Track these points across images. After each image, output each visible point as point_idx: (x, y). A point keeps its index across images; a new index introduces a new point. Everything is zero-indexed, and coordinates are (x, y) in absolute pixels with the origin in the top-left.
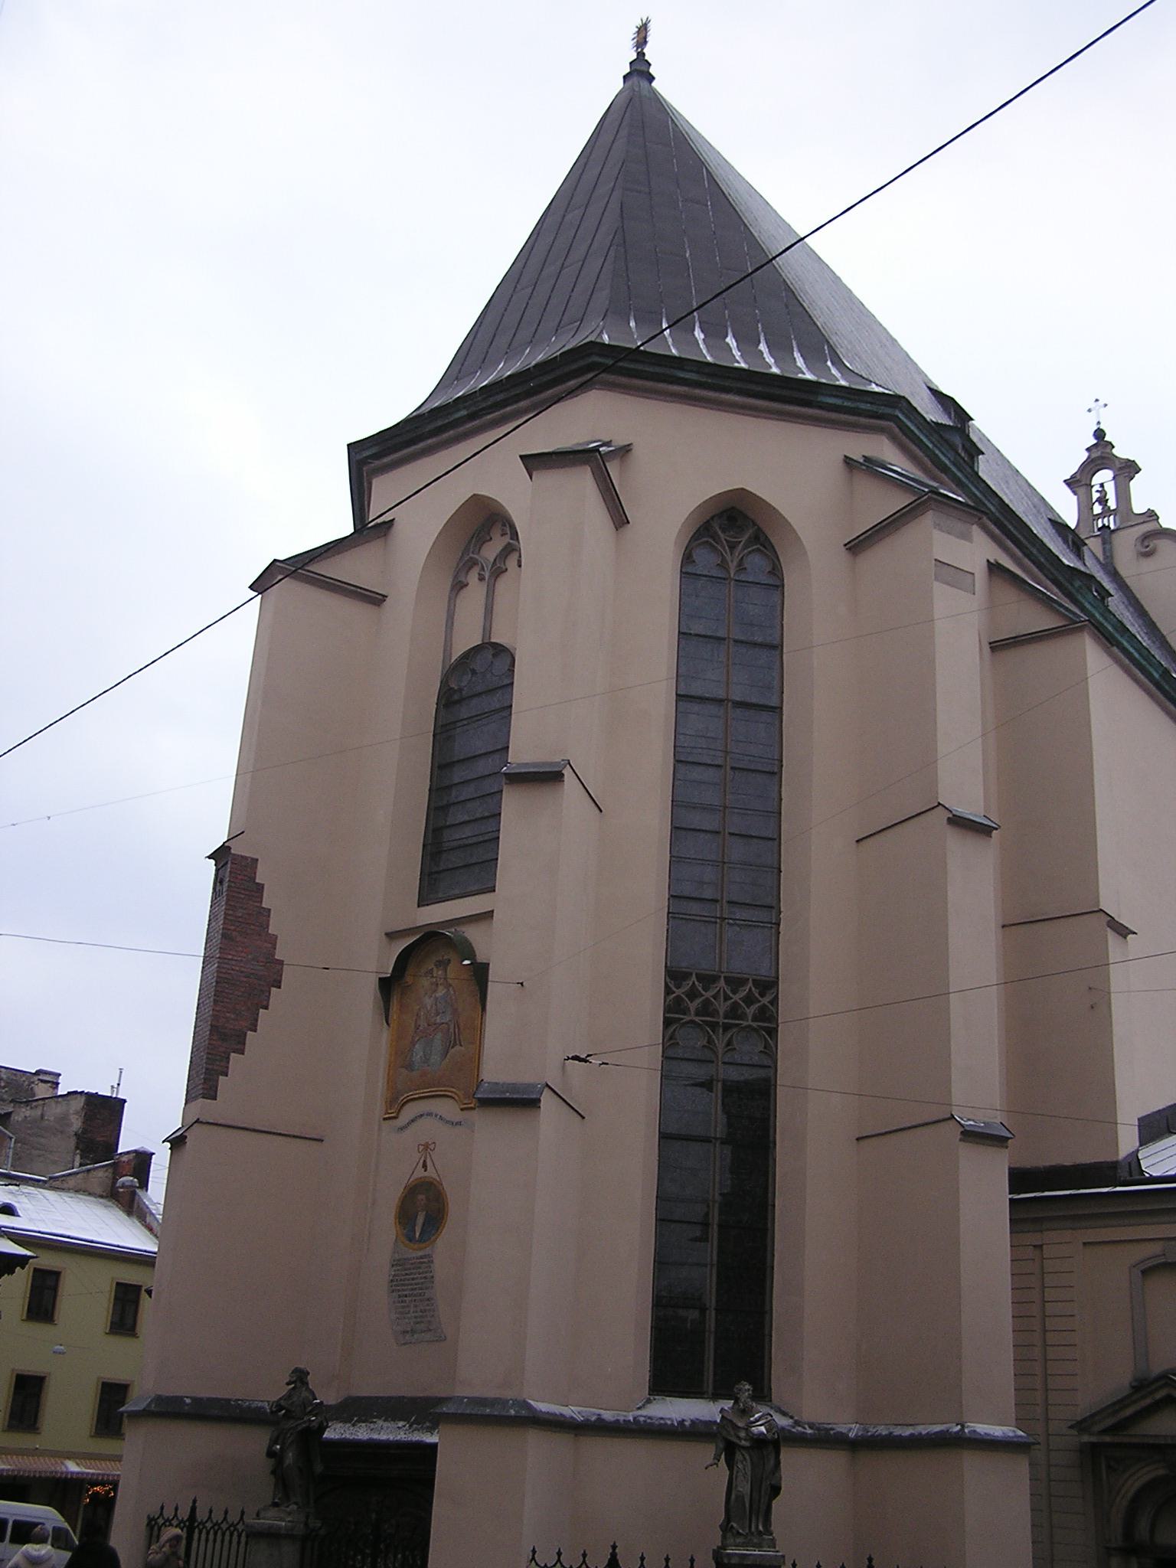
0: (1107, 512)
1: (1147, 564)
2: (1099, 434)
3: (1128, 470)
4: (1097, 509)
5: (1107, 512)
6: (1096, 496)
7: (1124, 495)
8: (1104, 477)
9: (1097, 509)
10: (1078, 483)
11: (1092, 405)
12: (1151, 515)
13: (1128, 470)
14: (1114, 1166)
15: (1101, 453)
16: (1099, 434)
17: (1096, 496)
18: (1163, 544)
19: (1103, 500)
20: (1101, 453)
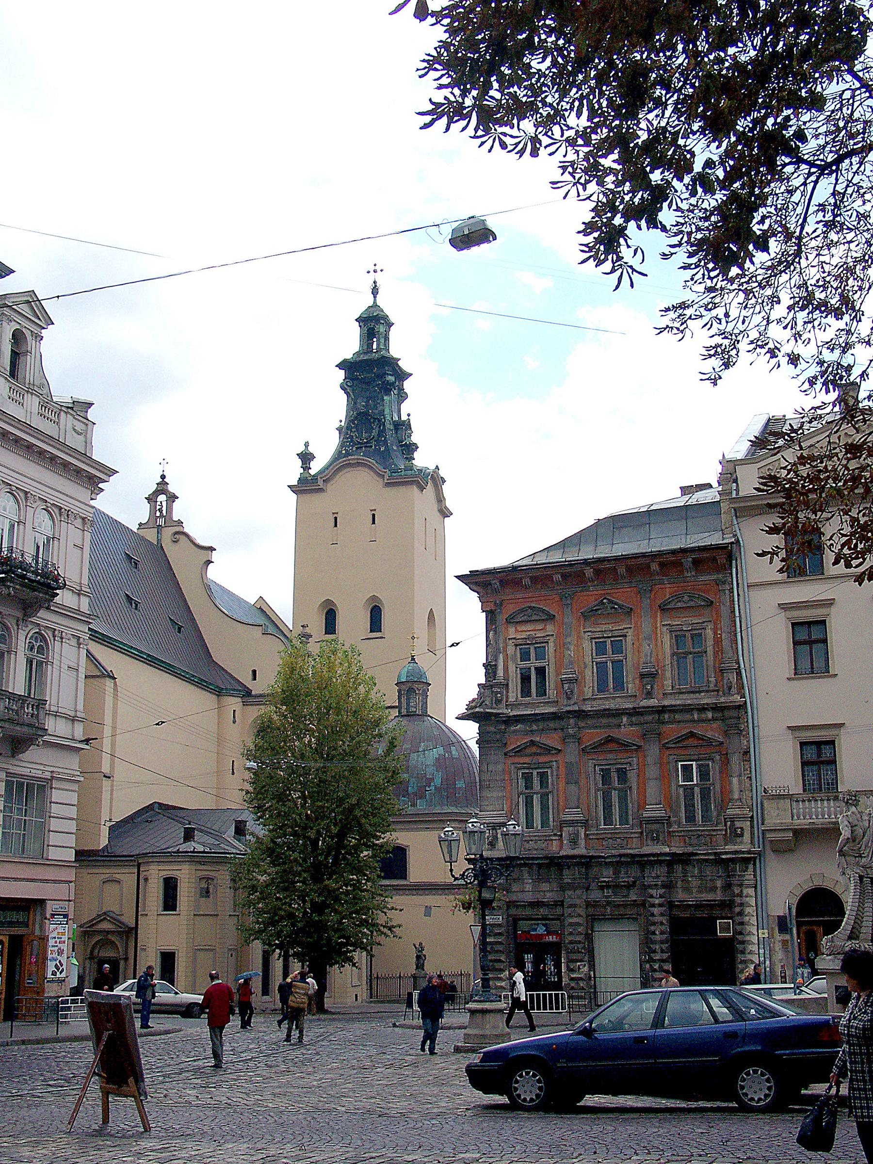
0: (161, 516)
1: (176, 547)
2: (163, 477)
3: (172, 498)
4: (158, 514)
5: (161, 516)
6: (158, 507)
7: (170, 509)
8: (162, 498)
9: (158, 514)
10: (151, 499)
11: (162, 462)
12: (180, 523)
13: (172, 498)
14: (99, 851)
15: (162, 487)
16: (163, 477)
17: (158, 507)
18: (183, 538)
19: (161, 510)
20: (162, 487)
